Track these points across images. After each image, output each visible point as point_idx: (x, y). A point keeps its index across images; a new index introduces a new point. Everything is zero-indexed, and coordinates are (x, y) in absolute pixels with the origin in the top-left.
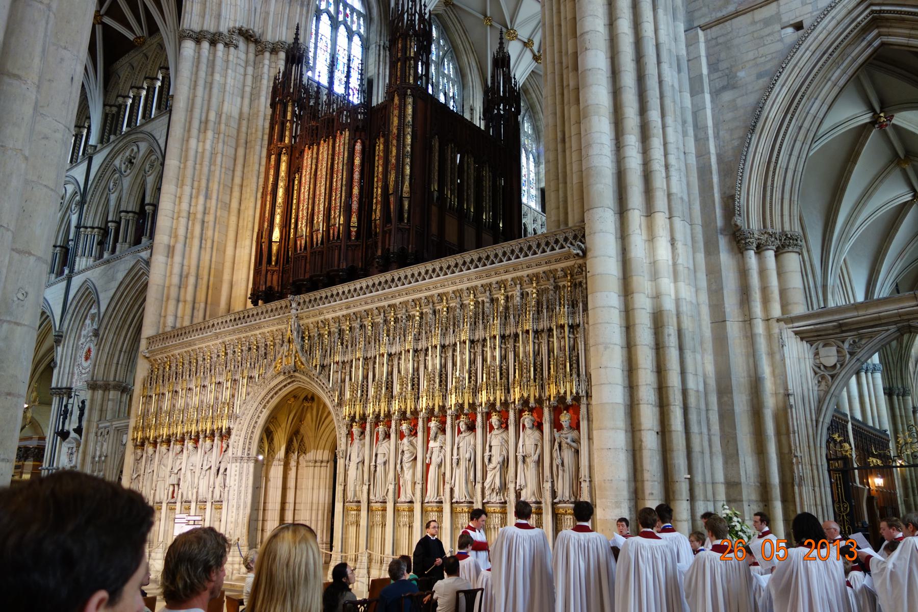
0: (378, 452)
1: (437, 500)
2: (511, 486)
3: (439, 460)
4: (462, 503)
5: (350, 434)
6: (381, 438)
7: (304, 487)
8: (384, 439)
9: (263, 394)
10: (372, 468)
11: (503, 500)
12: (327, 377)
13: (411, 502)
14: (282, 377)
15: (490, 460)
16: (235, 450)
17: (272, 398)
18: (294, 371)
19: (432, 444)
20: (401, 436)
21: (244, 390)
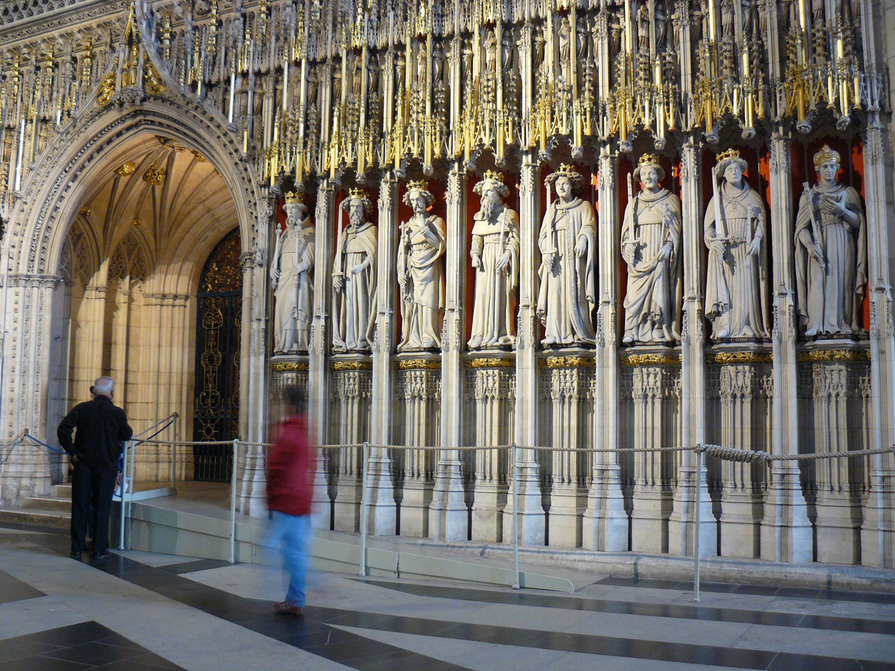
0: (349, 249)
1: (501, 341)
2: (692, 309)
3: (503, 259)
5: (279, 217)
6: (354, 219)
7: (141, 342)
8: (361, 224)
9: (72, 149)
10: (336, 282)
11: (668, 338)
12: (220, 105)
13: (435, 350)
14: (113, 115)
15: (638, 256)
16: (13, 263)
17: (90, 159)
18: (144, 100)
19: (481, 227)
20: (403, 212)
21: (30, 144)
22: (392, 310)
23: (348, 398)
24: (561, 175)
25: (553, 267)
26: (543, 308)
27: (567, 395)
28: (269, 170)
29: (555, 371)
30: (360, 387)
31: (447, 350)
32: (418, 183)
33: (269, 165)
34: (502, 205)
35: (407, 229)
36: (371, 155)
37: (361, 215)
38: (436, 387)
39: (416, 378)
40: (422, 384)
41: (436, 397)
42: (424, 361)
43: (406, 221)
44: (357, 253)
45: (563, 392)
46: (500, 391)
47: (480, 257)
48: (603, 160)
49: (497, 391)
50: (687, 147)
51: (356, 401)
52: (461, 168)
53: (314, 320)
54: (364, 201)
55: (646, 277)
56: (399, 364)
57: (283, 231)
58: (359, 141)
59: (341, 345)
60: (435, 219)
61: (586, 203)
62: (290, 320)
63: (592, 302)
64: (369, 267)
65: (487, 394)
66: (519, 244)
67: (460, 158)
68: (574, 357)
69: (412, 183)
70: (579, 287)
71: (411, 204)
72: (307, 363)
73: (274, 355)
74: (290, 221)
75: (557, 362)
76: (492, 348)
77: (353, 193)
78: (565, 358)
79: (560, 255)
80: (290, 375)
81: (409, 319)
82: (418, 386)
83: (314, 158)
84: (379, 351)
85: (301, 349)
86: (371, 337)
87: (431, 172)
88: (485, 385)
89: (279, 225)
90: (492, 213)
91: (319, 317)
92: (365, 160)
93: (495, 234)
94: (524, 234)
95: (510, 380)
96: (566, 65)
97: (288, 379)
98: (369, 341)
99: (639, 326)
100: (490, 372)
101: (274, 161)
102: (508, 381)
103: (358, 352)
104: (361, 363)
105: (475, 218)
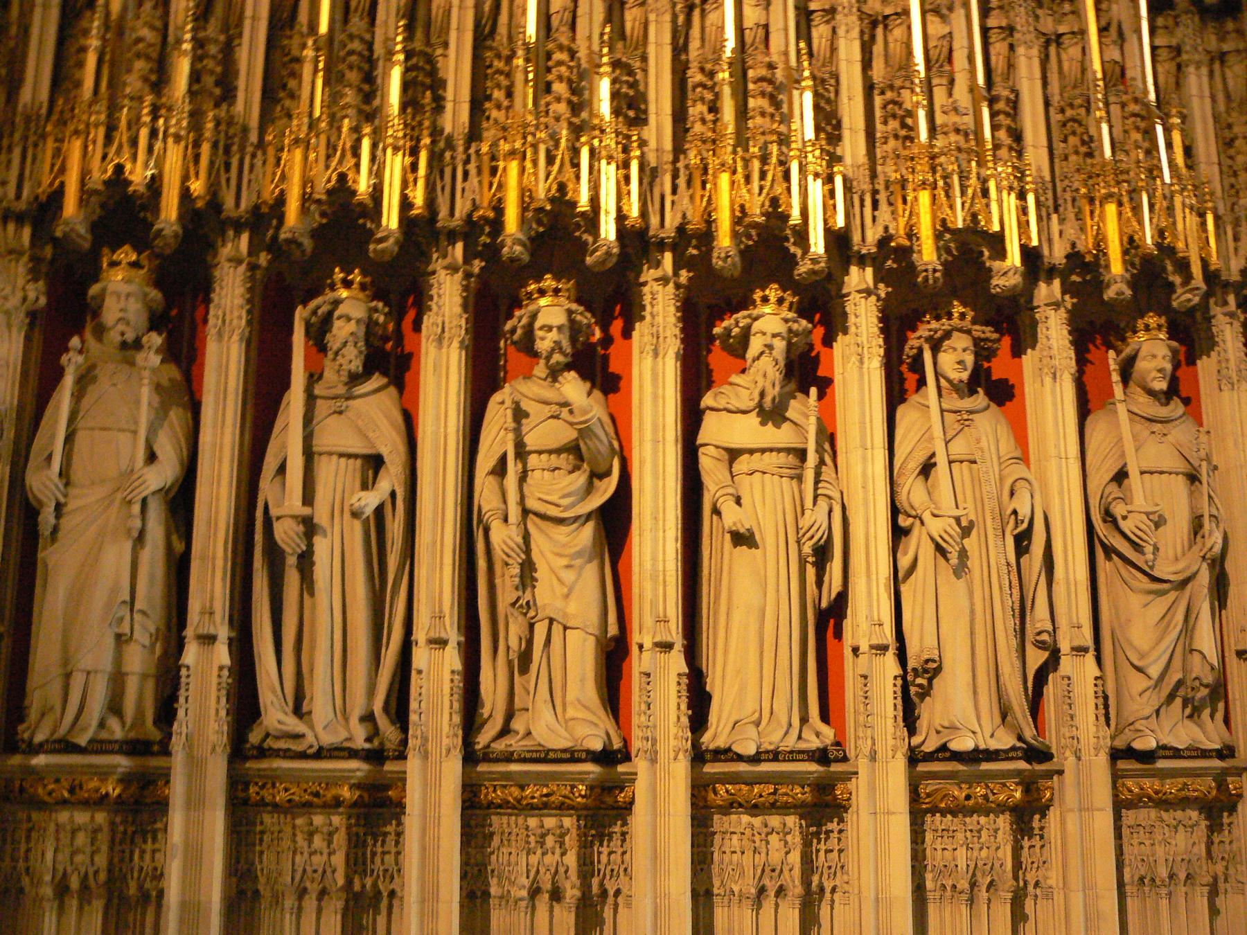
13: (608, 757)
23: (302, 893)
24: (960, 330)
33: (57, 152)
38: (592, 863)
39: (543, 836)
40: (563, 854)
44: (349, 456)
50: (1225, 314)
54: (376, 310)
55: (1172, 596)
56: (476, 794)
58: (390, 141)
65: (766, 882)
69: (549, 282)
75: (968, 797)
77: (347, 284)
80: (81, 817)
83: (219, 162)
85: (132, 735)
90: (780, 395)
91: (208, 640)
95: (815, 841)
96: (944, 81)
98: (383, 722)
99: (1158, 712)
100: (775, 821)
103: (352, 754)
104: (358, 786)
105: (703, 404)
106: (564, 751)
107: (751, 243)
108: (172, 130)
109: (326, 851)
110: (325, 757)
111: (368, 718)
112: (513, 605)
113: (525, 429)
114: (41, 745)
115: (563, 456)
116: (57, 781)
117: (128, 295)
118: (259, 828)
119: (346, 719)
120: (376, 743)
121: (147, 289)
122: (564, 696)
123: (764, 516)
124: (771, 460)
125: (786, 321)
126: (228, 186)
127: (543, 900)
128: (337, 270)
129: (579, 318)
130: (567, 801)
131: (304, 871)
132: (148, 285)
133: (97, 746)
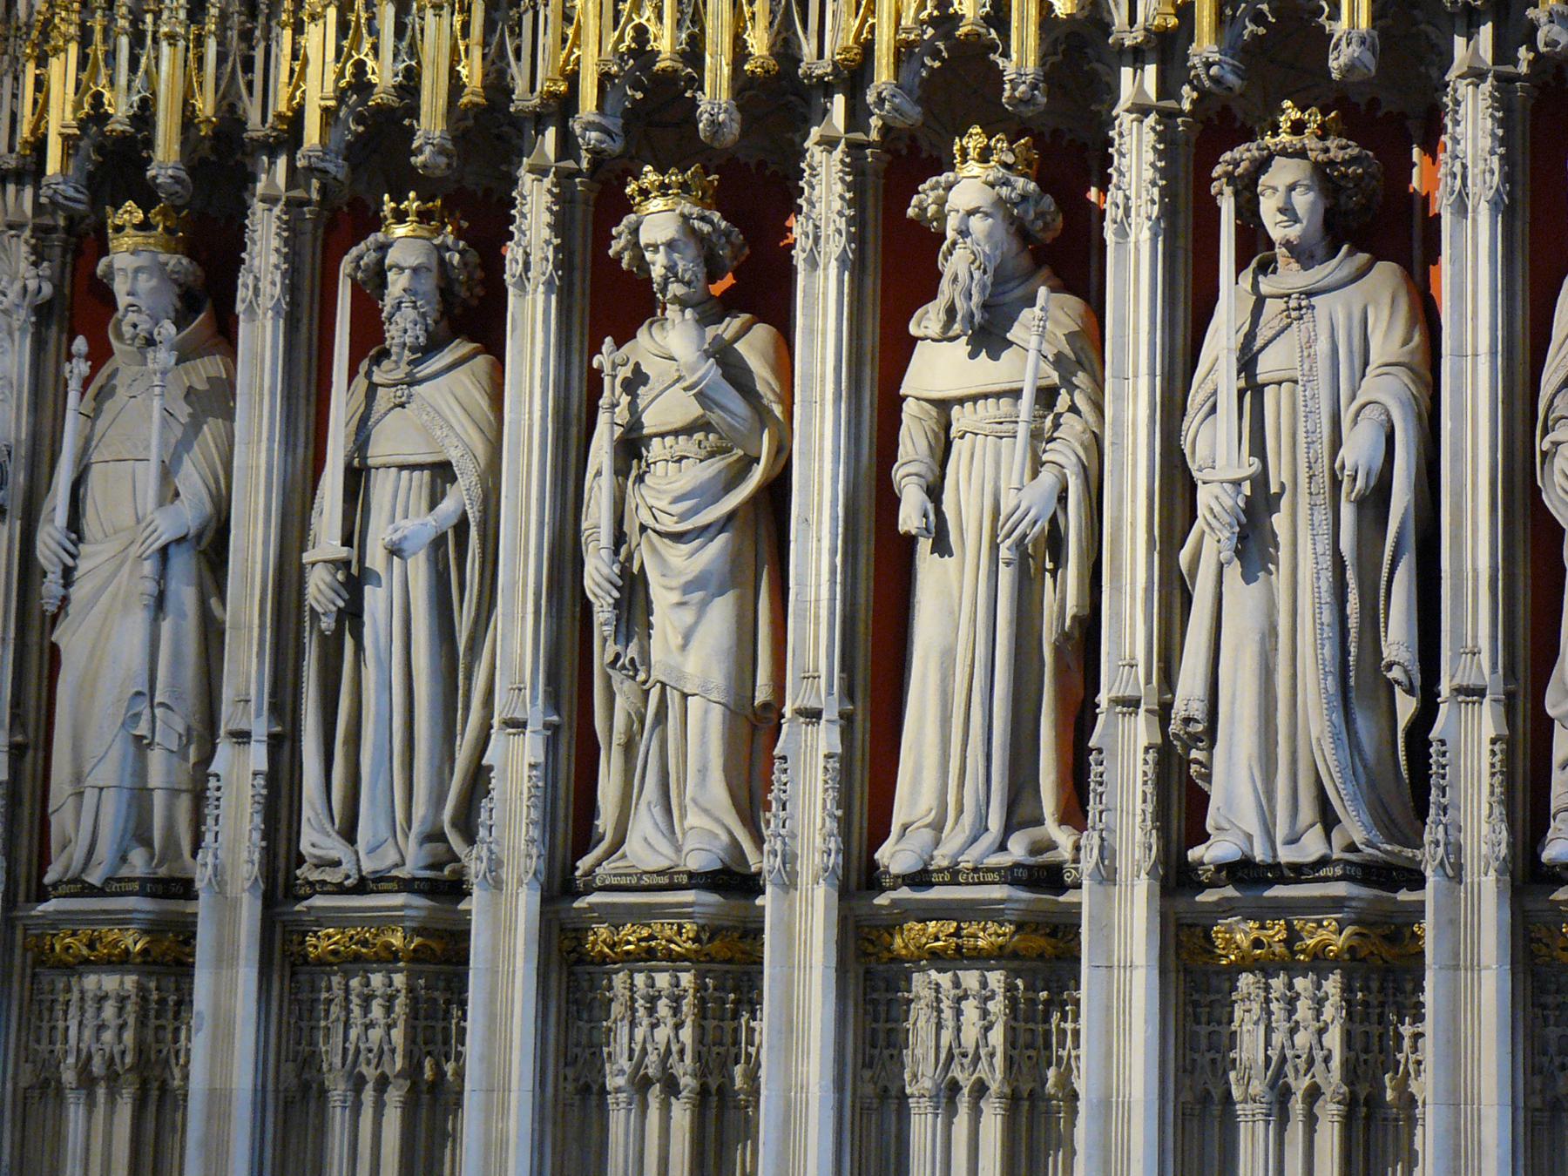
0: (378, 452)
1: (1018, 849)
4: (1299, 873)
6: (403, 327)
10: (320, 588)
22: (558, 711)
23: (359, 1083)
24: (1283, 152)
25: (1242, 538)
26: (1198, 710)
27: (1300, 1085)
28: (41, 109)
29: (1246, 981)
30: (411, 1039)
31: (789, 883)
32: (674, 178)
34: (1028, 276)
35: (625, 372)
36: (477, 53)
37: (431, 307)
38: (736, 1043)
39: (652, 1001)
40: (678, 1026)
41: (739, 1082)
42: (690, 928)
43: (624, 336)
45: (1280, 1073)
46: (1010, 1062)
47: (934, 492)
48: (1465, 90)
49: (999, 1061)
51: (394, 1096)
52: (856, 116)
53: (224, 749)
57: (95, 370)
59: (334, 854)
60: (745, 330)
61: (1386, 273)
62: (117, 746)
63: (1410, 691)
64: (462, 527)
65: (956, 1072)
66: (1098, 440)
67: (855, 75)
68: (1330, 921)
69: (650, 176)
70: (1353, 623)
71: (644, 266)
72: (185, 932)
73: (43, 896)
74: (127, 330)
75: (1257, 943)
76: (980, 874)
77: (400, 217)
78: (1289, 927)
79: (1274, 489)
80: (110, 982)
81: (629, 748)
82: (662, 1034)
83: (234, 59)
84: (498, 884)
85: (162, 872)
86: (467, 824)
87: (733, 130)
88: (947, 1036)
89: (80, 344)
90: (985, 306)
91: (242, 737)
92: (454, 75)
93: (998, 395)
94: (1119, 398)
95: (1056, 1017)
97: (101, 999)
100: (970, 979)
101: (62, 71)
102: (1047, 1020)
103: (407, 885)
104: (418, 932)
105: (913, 329)
106: (660, 873)
107: (937, 64)
108: (164, 29)
109: (382, 1022)
110: (372, 892)
111: (435, 836)
112: (613, 664)
113: (641, 403)
114: (55, 885)
115: (699, 436)
116: (74, 934)
117: (137, 270)
118: (324, 995)
119: (407, 836)
120: (447, 871)
121: (163, 257)
122: (682, 794)
123: (968, 505)
124: (988, 409)
125: (992, 186)
126: (251, 93)
127: (655, 1094)
128: (386, 197)
129: (697, 224)
130: (672, 946)
131: (358, 1051)
132: (168, 251)
133: (115, 886)
